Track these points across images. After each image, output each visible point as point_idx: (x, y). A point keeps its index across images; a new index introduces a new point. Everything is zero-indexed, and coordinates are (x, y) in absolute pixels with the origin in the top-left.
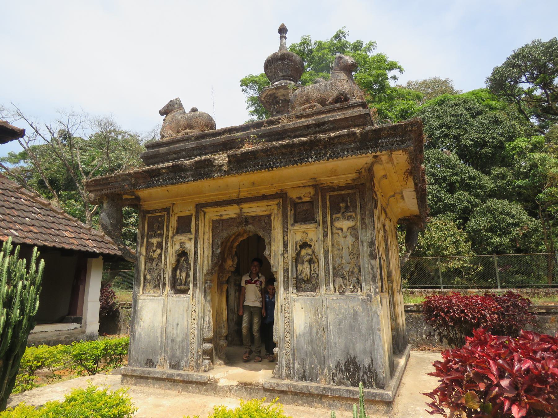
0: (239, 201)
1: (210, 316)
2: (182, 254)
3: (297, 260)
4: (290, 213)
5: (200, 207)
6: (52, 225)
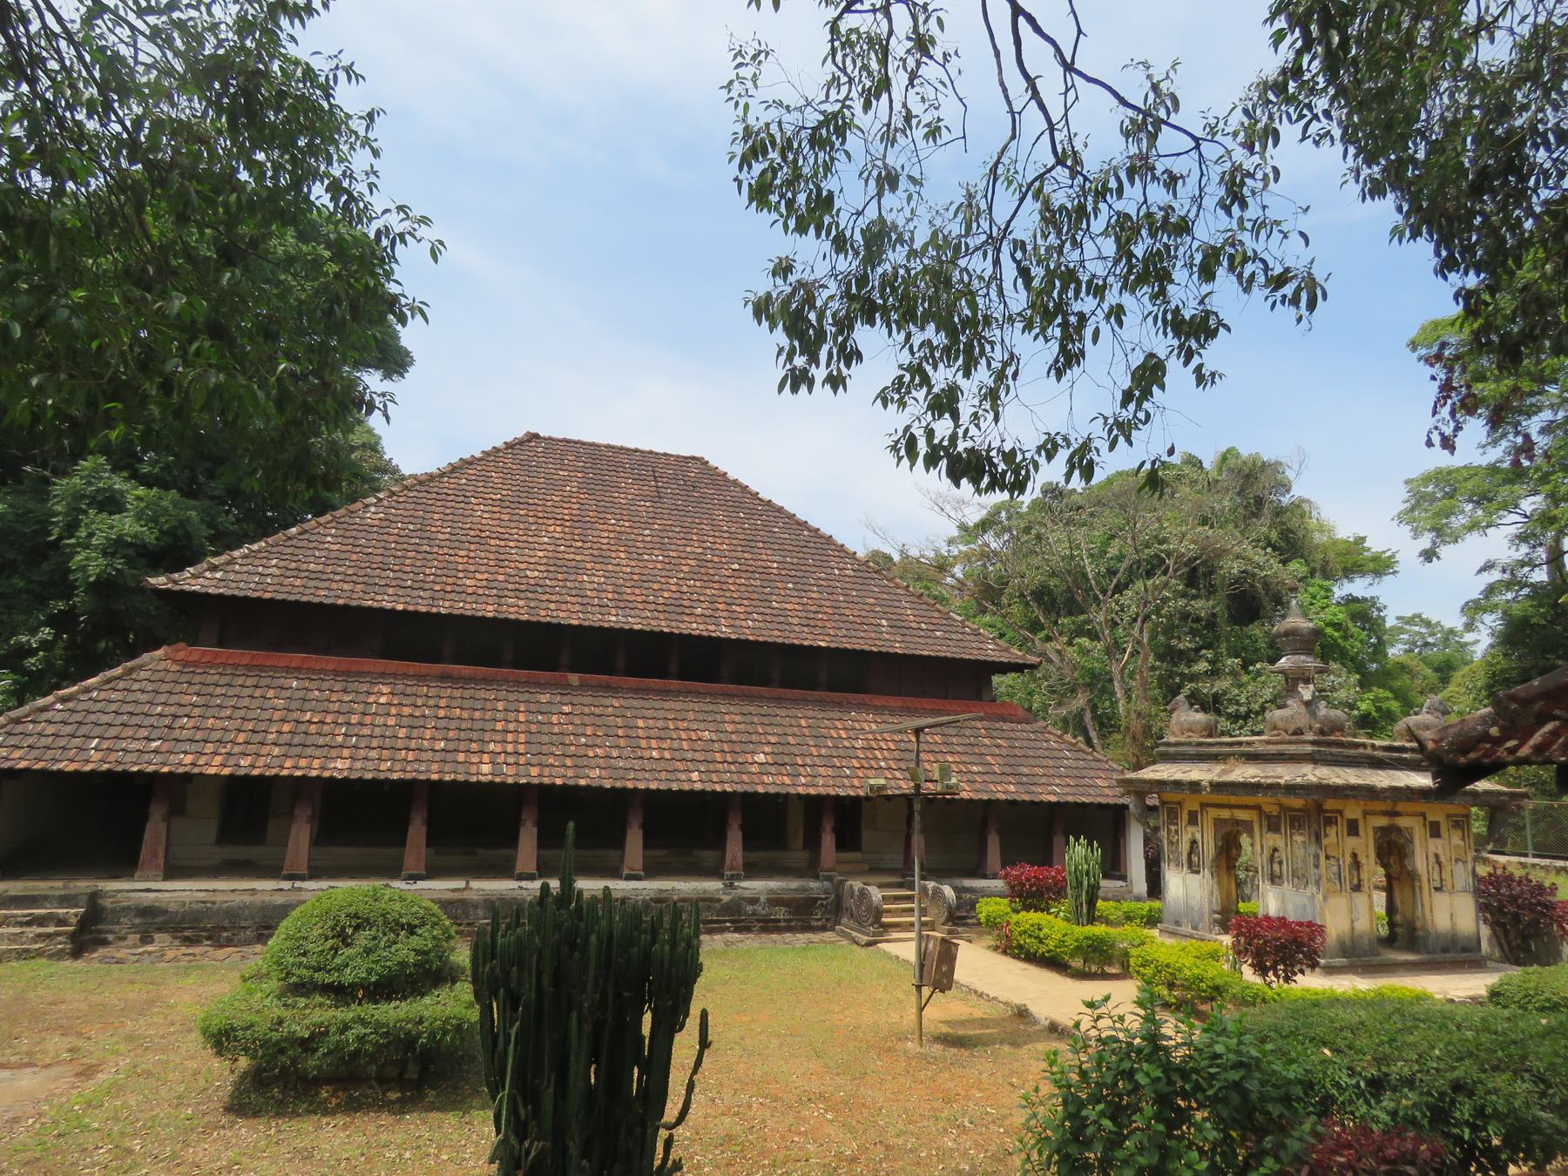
0: (1231, 807)
1: (1216, 893)
2: (1194, 842)
4: (1265, 823)
5: (1204, 805)
6: (1085, 773)
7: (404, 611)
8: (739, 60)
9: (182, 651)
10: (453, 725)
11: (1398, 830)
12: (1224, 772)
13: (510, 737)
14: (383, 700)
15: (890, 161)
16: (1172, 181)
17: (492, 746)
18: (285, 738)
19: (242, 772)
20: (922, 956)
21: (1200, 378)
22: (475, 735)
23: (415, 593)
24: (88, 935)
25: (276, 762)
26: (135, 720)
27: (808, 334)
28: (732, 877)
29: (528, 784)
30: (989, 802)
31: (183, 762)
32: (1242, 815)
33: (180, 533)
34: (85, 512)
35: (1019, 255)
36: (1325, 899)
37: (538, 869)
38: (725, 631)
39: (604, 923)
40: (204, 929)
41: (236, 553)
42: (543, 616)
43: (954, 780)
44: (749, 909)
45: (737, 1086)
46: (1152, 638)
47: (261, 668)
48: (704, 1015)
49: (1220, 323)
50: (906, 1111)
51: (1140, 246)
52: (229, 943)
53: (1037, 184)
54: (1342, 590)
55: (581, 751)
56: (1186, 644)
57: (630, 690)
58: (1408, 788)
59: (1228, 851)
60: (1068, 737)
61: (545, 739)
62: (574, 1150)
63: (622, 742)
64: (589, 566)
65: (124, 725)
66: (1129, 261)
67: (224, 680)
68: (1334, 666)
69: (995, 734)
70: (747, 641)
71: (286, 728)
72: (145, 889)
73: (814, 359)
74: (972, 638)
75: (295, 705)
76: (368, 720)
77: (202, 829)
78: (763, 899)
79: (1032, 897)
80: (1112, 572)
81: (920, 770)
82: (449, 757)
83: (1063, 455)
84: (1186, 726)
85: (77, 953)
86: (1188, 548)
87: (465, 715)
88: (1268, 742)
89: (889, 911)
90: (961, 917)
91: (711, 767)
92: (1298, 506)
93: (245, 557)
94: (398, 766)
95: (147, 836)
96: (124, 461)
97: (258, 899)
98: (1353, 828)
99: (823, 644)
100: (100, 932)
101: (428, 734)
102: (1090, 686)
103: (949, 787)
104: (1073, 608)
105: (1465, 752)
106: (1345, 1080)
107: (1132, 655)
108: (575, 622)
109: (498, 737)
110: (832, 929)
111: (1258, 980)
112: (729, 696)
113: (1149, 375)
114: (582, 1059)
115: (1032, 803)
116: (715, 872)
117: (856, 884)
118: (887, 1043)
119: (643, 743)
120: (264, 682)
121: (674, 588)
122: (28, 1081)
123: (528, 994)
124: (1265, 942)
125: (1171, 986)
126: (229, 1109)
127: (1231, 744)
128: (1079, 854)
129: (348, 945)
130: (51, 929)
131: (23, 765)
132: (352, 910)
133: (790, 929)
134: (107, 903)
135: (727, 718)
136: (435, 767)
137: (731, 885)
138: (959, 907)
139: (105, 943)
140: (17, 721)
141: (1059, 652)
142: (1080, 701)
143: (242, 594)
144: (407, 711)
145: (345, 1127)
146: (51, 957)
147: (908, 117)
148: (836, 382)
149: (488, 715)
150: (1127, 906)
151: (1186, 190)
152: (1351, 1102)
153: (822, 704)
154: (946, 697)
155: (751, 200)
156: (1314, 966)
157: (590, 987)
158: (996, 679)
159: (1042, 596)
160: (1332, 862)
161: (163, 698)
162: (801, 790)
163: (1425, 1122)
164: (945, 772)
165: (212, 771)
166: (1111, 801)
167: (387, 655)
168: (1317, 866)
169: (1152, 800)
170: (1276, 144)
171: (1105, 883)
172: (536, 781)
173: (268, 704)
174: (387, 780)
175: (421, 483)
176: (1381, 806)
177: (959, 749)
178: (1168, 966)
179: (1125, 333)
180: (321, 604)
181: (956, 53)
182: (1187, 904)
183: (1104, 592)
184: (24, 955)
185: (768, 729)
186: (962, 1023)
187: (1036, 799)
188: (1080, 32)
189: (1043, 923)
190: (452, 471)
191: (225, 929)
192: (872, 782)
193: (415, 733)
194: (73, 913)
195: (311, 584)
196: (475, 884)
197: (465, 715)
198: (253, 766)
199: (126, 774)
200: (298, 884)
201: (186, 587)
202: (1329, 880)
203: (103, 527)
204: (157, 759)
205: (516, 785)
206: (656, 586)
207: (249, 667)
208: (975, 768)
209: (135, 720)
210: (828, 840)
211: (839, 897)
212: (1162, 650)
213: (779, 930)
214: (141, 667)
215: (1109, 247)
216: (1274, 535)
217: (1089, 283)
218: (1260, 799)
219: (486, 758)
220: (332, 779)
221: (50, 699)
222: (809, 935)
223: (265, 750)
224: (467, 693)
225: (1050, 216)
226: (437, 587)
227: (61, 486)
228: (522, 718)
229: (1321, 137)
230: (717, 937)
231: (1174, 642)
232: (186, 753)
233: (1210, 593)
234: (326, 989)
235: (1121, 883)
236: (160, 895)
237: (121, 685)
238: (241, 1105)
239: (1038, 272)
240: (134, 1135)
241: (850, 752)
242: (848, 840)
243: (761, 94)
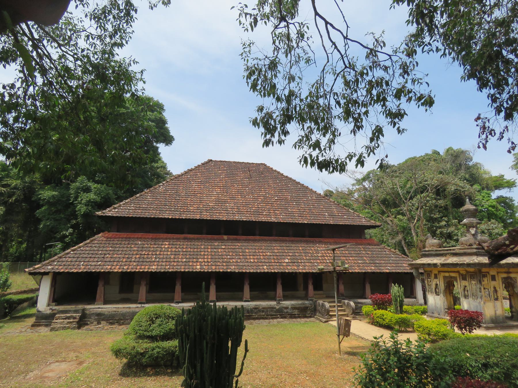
1: (446, 302)
2: (437, 285)
3: (464, 290)
4: (461, 277)
5: (439, 272)
6: (399, 262)
7: (172, 218)
8: (244, 46)
9: (107, 234)
10: (188, 253)
11: (511, 278)
12: (445, 260)
13: (206, 257)
14: (166, 247)
15: (292, 73)
16: (386, 69)
17: (200, 260)
18: (137, 260)
19: (125, 271)
20: (339, 325)
21: (399, 131)
22: (195, 257)
23: (175, 212)
24: (82, 322)
25: (135, 267)
26: (93, 256)
27: (270, 127)
28: (280, 300)
29: (212, 272)
30: (365, 273)
31: (107, 268)
32: (453, 275)
33: (107, 197)
34: (80, 193)
35: (336, 97)
36: (484, 303)
37: (216, 299)
38: (273, 220)
39: (213, 313)
40: (116, 320)
41: (121, 203)
42: (215, 218)
43: (346, 266)
44: (285, 311)
45: (278, 368)
46: (425, 214)
47: (130, 238)
48: (246, 342)
49: (405, 113)
50: (333, 377)
51: (374, 90)
52: (123, 324)
53: (342, 73)
54: (495, 194)
55: (228, 260)
56: (437, 216)
57: (243, 240)
58: (513, 263)
59: (449, 287)
60: (393, 250)
61: (217, 257)
62: (207, 384)
63: (241, 257)
64: (229, 201)
65: (90, 257)
66: (371, 96)
67: (119, 242)
68: (493, 221)
69: (367, 250)
70: (281, 222)
71: (137, 256)
72: (92, 308)
73: (273, 135)
74: (357, 217)
75: (140, 249)
76: (162, 253)
77: (114, 289)
78: (290, 307)
79: (381, 305)
80: (408, 192)
81: (335, 263)
82: (187, 264)
83: (354, 159)
84: (431, 244)
85: (79, 328)
86: (435, 182)
87: (192, 250)
88: (460, 249)
89: (332, 311)
90: (357, 313)
91: (271, 264)
92: (476, 166)
93: (124, 204)
94: (171, 267)
95: (98, 291)
96: (91, 177)
97: (131, 310)
98: (493, 278)
99: (306, 222)
100: (86, 321)
101: (180, 257)
102: (403, 232)
103: (345, 268)
104: (396, 206)
105: (497, 250)
106: (474, 364)
107: (418, 221)
108: (225, 219)
109: (202, 257)
110: (314, 317)
111: (460, 332)
112: (275, 240)
113: (378, 132)
114: (208, 355)
115: (380, 273)
116: (273, 299)
117: (321, 302)
118: (329, 355)
119: (248, 257)
120: (131, 242)
121: (256, 206)
122: (64, 366)
123: (192, 335)
124: (461, 319)
125: (429, 334)
126: (120, 375)
127: (447, 250)
128: (396, 290)
129: (153, 323)
130: (72, 320)
131: (62, 271)
132: (155, 312)
133: (299, 317)
134: (87, 312)
135: (275, 248)
136: (183, 267)
137: (279, 303)
138: (356, 309)
139: (87, 324)
140: (60, 257)
141: (391, 221)
142: (400, 237)
143: (123, 216)
144: (174, 250)
145: (154, 380)
146: (72, 329)
147: (299, 57)
148: (280, 142)
149: (199, 250)
150: (415, 307)
151: (391, 72)
152: (476, 372)
153: (307, 242)
154: (349, 238)
155: (251, 89)
156: (479, 327)
157: (209, 333)
158: (366, 231)
159: (384, 202)
160: (486, 290)
161: (101, 249)
162: (300, 271)
163: (503, 379)
164: (343, 263)
165: (116, 271)
166: (409, 271)
167: (167, 232)
168: (481, 292)
169: (421, 271)
170: (415, 55)
171: (406, 300)
172: (214, 271)
173: (132, 249)
174: (168, 272)
175: (176, 178)
176: (504, 270)
177: (354, 255)
178: (427, 328)
179: (369, 119)
180: (147, 217)
181: (311, 37)
182: (436, 306)
183: (406, 199)
184: (64, 328)
185: (289, 251)
186: (356, 348)
187: (382, 271)
188: (348, 27)
189: (384, 314)
190: (185, 174)
191: (122, 320)
192: (319, 267)
193: (176, 256)
194: (78, 315)
195: (144, 211)
197: (192, 250)
198: (128, 269)
199: (91, 273)
200: (143, 305)
201: (107, 215)
202: (485, 296)
203: (85, 197)
204: (100, 267)
205: (208, 272)
206: (250, 206)
207: (126, 238)
208: (360, 262)
209: (93, 256)
210: (311, 287)
211: (315, 306)
212: (428, 218)
213: (295, 318)
214: (95, 240)
215: (364, 93)
216: (467, 176)
217: (362, 103)
218: (458, 269)
219: (198, 264)
220: (151, 272)
221: (69, 250)
222: (306, 319)
223: (131, 264)
224: (192, 243)
225: (347, 83)
226: (182, 210)
227: (73, 185)
228: (209, 251)
229: (430, 51)
230: (275, 320)
231: (432, 215)
232: (108, 265)
233: (445, 198)
234: (148, 337)
235: (414, 300)
236: (102, 309)
237: (89, 245)
238: (124, 374)
239: (342, 102)
240: (93, 382)
241: (317, 258)
242: (318, 287)
243: (252, 56)
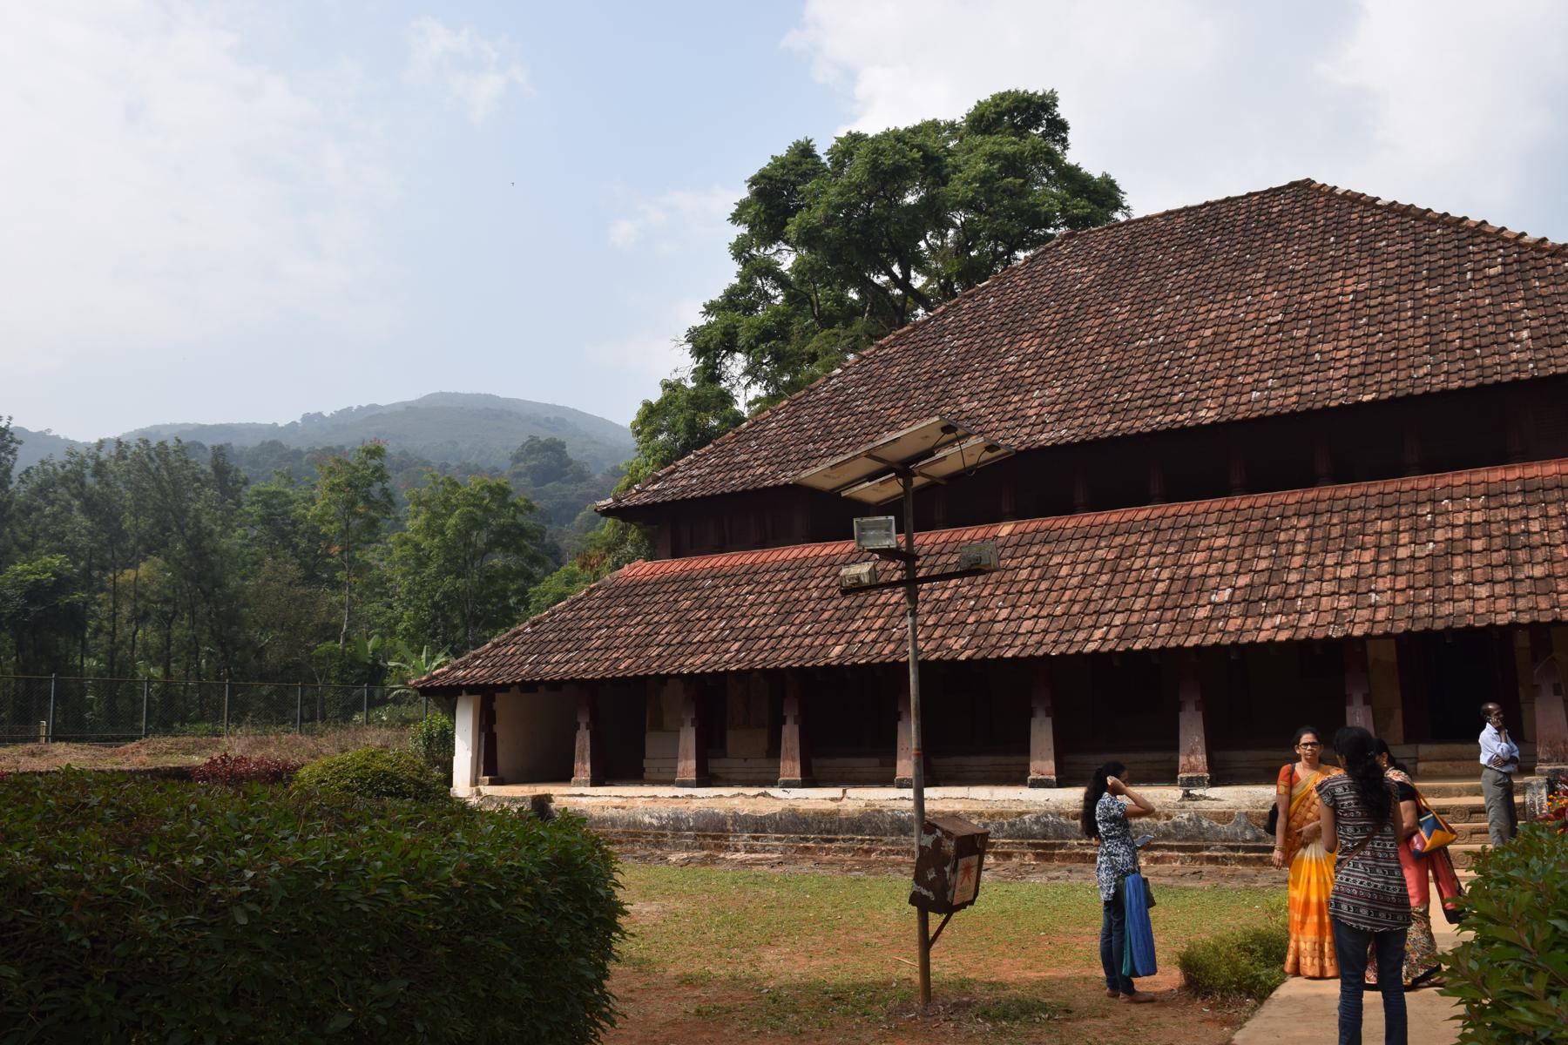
28: (1191, 782)
38: (1207, 415)
41: (680, 463)
144: (796, 594)
196: (853, 792)
